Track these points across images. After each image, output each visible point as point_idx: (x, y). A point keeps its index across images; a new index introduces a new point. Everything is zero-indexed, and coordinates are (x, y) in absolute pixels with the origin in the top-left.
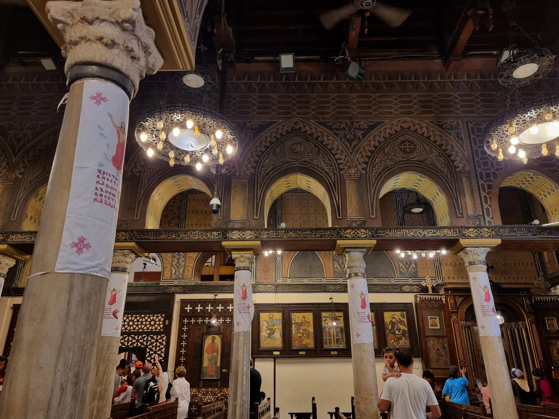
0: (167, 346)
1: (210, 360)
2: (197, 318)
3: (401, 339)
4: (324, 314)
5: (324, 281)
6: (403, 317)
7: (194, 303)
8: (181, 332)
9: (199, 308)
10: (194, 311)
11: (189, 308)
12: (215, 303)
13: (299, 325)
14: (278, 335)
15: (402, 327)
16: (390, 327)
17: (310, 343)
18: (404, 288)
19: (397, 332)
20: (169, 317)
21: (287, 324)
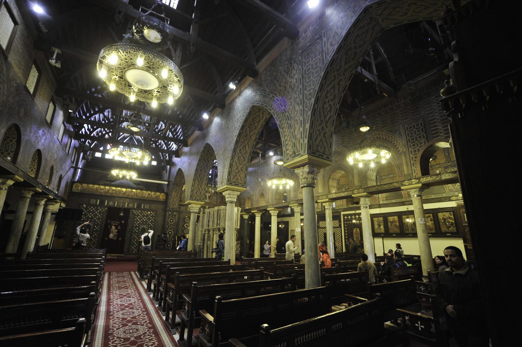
0: (341, 232)
1: (356, 238)
2: (349, 221)
3: (450, 227)
4: (404, 217)
5: (403, 200)
6: (451, 215)
7: (347, 215)
8: (344, 227)
9: (349, 217)
10: (348, 218)
11: (346, 217)
12: (355, 215)
13: (391, 222)
14: (382, 227)
15: (451, 221)
16: (443, 221)
17: (397, 230)
18: (452, 198)
19: (447, 224)
20: (340, 221)
21: (386, 221)
